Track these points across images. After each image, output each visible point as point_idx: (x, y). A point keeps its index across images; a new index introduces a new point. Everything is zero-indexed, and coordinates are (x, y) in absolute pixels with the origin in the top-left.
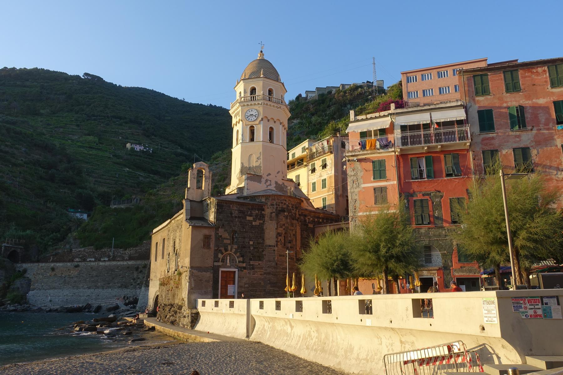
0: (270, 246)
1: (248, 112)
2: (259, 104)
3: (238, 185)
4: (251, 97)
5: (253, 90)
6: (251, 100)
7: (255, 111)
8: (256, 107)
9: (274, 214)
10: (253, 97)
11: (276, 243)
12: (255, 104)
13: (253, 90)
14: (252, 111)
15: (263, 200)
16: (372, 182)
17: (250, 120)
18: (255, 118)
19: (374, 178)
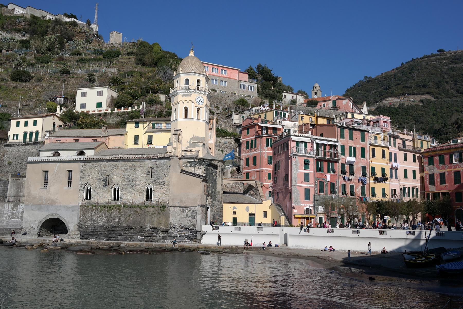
0: (218, 192)
1: (197, 97)
2: (202, 94)
3: (188, 147)
4: (197, 87)
5: (198, 81)
6: (197, 89)
7: (202, 98)
8: (202, 95)
9: (220, 172)
10: (199, 87)
11: (220, 190)
12: (202, 94)
13: (198, 81)
14: (200, 97)
15: (216, 162)
16: (303, 170)
17: (199, 104)
18: (202, 104)
19: (304, 168)
